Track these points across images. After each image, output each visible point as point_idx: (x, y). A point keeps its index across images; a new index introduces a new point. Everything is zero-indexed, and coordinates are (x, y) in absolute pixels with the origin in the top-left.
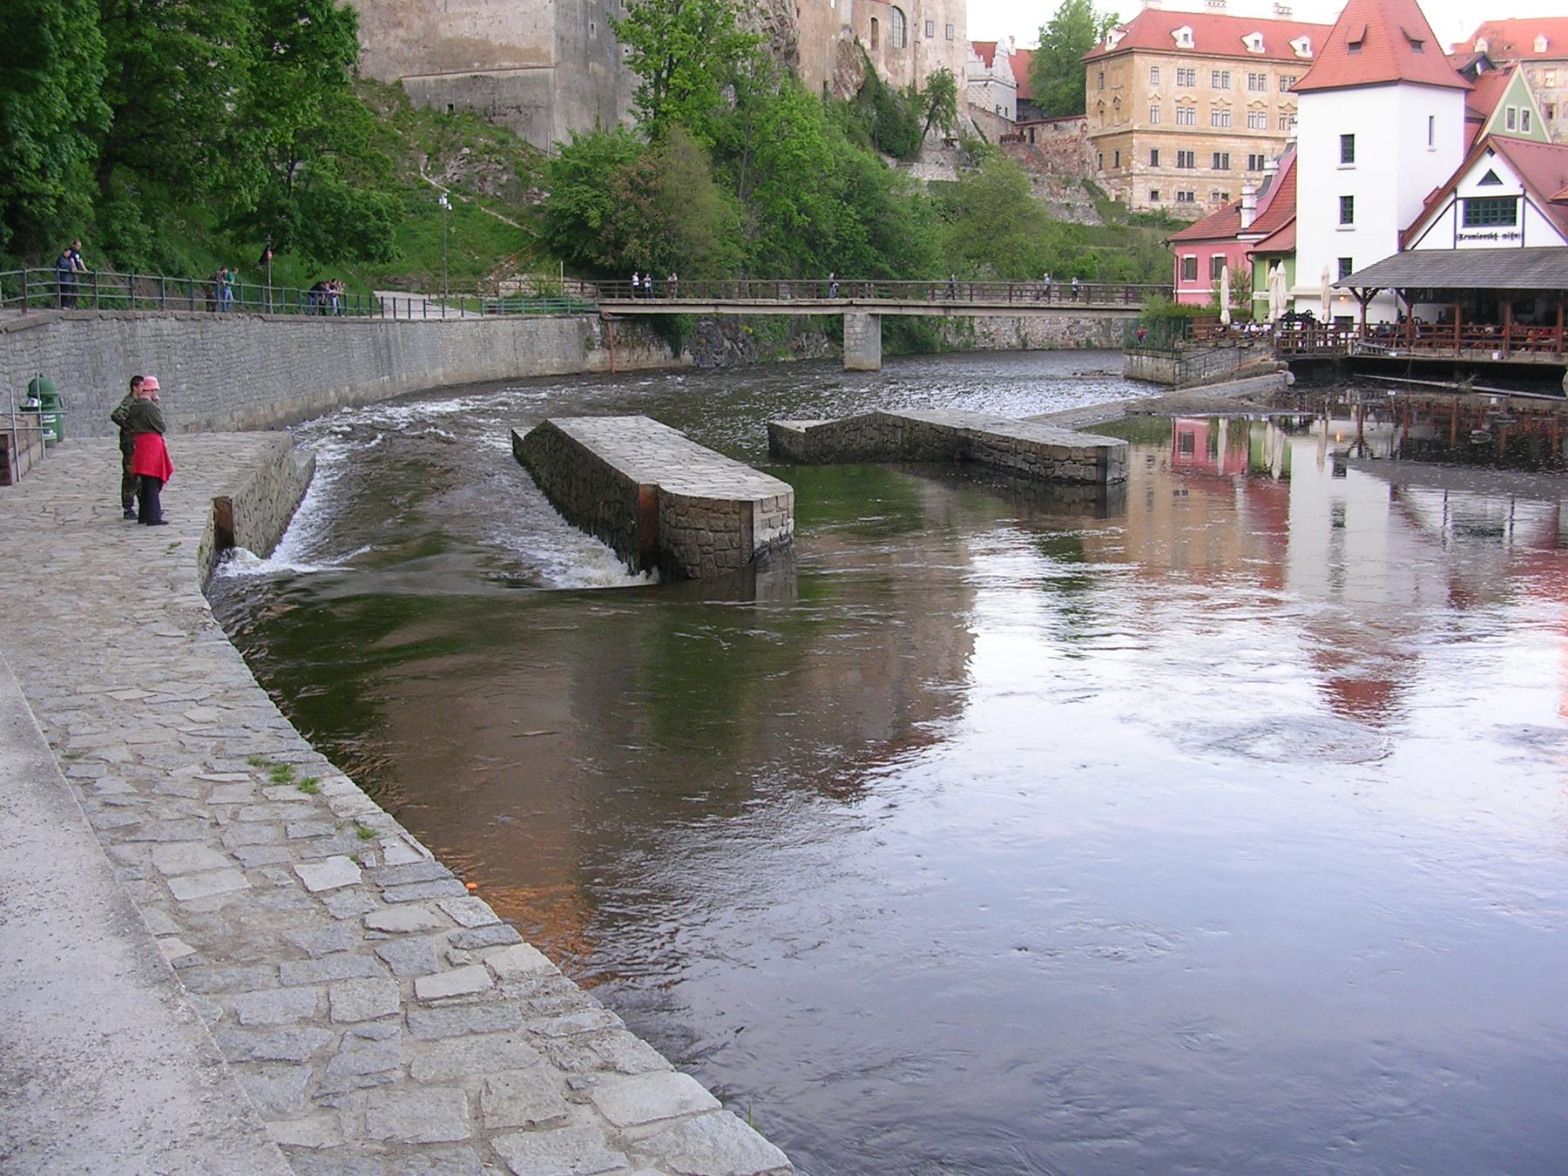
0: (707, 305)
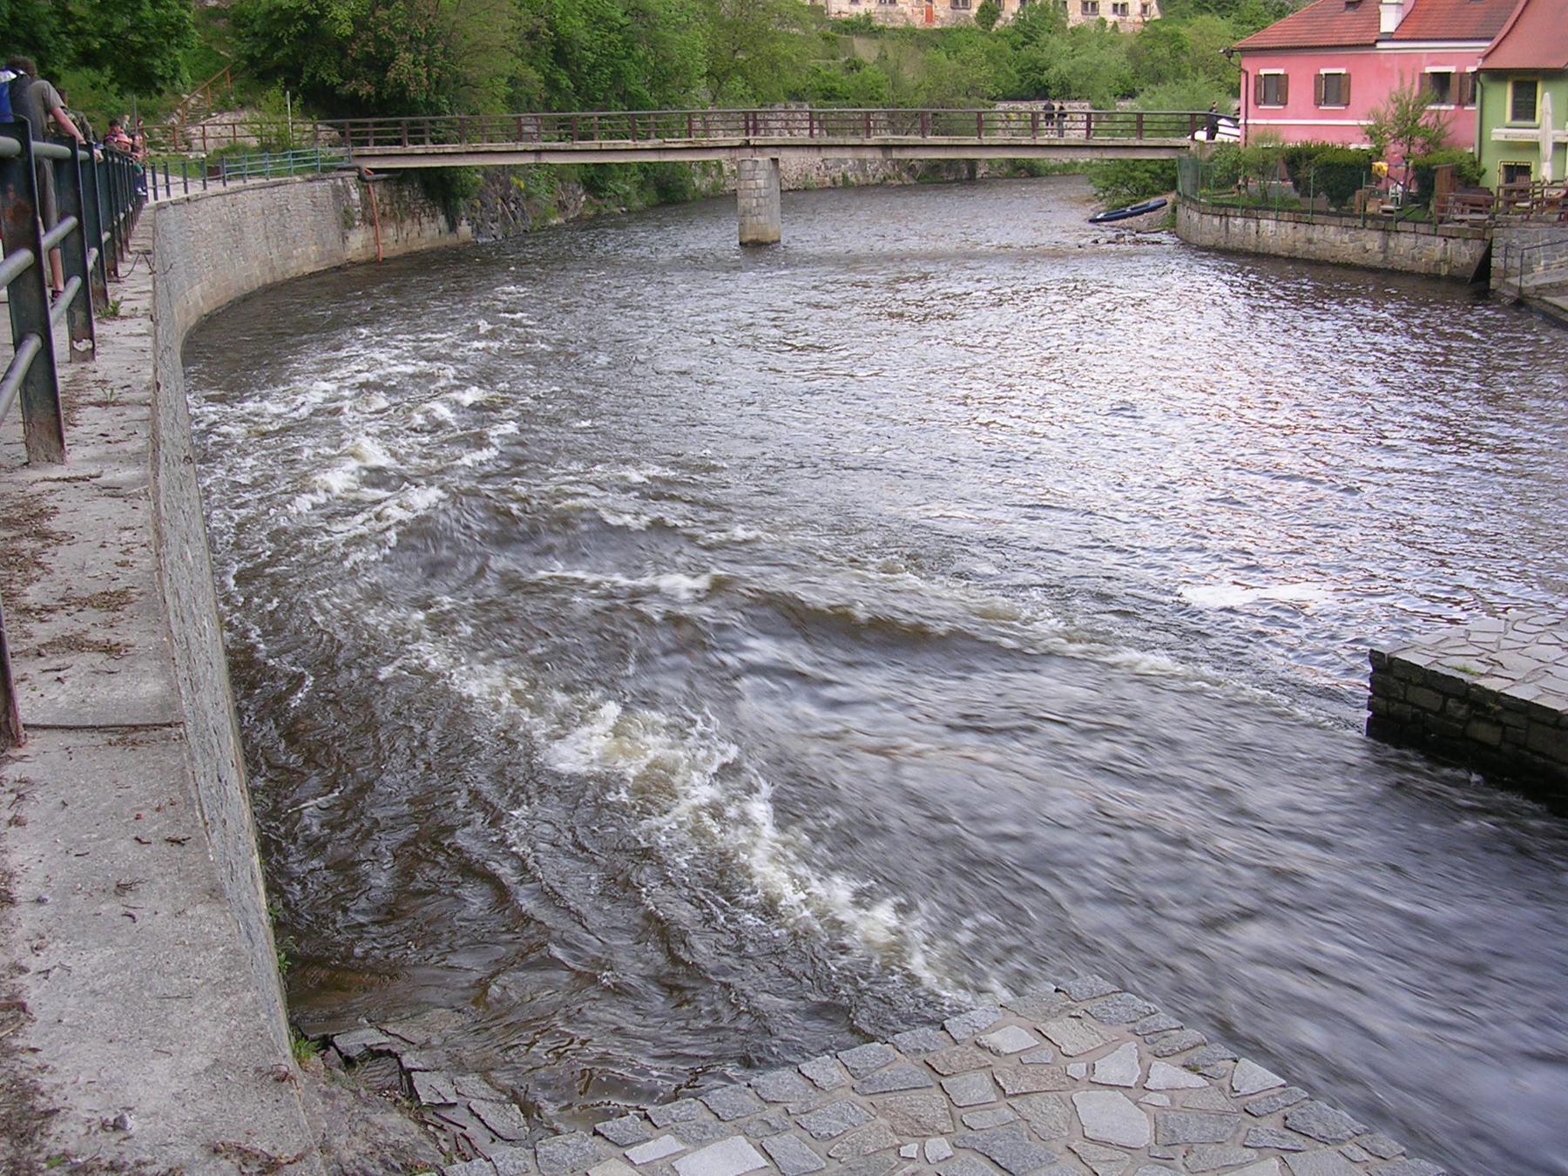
0: (525, 151)
